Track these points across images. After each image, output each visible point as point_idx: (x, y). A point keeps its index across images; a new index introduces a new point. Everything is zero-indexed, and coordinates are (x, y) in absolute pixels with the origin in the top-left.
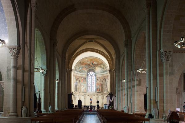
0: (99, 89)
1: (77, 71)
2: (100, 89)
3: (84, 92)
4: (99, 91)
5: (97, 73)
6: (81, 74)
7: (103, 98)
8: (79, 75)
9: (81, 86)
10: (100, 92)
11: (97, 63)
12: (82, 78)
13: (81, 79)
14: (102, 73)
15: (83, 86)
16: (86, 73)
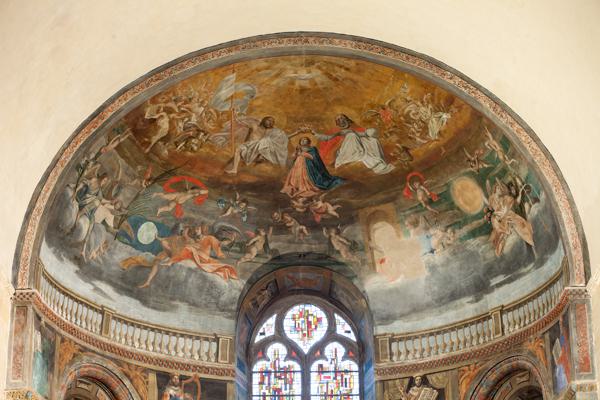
1: (89, 271)
5: (388, 319)
8: (119, 336)
11: (386, 155)
12: (164, 379)
14: (467, 308)
16: (222, 309)
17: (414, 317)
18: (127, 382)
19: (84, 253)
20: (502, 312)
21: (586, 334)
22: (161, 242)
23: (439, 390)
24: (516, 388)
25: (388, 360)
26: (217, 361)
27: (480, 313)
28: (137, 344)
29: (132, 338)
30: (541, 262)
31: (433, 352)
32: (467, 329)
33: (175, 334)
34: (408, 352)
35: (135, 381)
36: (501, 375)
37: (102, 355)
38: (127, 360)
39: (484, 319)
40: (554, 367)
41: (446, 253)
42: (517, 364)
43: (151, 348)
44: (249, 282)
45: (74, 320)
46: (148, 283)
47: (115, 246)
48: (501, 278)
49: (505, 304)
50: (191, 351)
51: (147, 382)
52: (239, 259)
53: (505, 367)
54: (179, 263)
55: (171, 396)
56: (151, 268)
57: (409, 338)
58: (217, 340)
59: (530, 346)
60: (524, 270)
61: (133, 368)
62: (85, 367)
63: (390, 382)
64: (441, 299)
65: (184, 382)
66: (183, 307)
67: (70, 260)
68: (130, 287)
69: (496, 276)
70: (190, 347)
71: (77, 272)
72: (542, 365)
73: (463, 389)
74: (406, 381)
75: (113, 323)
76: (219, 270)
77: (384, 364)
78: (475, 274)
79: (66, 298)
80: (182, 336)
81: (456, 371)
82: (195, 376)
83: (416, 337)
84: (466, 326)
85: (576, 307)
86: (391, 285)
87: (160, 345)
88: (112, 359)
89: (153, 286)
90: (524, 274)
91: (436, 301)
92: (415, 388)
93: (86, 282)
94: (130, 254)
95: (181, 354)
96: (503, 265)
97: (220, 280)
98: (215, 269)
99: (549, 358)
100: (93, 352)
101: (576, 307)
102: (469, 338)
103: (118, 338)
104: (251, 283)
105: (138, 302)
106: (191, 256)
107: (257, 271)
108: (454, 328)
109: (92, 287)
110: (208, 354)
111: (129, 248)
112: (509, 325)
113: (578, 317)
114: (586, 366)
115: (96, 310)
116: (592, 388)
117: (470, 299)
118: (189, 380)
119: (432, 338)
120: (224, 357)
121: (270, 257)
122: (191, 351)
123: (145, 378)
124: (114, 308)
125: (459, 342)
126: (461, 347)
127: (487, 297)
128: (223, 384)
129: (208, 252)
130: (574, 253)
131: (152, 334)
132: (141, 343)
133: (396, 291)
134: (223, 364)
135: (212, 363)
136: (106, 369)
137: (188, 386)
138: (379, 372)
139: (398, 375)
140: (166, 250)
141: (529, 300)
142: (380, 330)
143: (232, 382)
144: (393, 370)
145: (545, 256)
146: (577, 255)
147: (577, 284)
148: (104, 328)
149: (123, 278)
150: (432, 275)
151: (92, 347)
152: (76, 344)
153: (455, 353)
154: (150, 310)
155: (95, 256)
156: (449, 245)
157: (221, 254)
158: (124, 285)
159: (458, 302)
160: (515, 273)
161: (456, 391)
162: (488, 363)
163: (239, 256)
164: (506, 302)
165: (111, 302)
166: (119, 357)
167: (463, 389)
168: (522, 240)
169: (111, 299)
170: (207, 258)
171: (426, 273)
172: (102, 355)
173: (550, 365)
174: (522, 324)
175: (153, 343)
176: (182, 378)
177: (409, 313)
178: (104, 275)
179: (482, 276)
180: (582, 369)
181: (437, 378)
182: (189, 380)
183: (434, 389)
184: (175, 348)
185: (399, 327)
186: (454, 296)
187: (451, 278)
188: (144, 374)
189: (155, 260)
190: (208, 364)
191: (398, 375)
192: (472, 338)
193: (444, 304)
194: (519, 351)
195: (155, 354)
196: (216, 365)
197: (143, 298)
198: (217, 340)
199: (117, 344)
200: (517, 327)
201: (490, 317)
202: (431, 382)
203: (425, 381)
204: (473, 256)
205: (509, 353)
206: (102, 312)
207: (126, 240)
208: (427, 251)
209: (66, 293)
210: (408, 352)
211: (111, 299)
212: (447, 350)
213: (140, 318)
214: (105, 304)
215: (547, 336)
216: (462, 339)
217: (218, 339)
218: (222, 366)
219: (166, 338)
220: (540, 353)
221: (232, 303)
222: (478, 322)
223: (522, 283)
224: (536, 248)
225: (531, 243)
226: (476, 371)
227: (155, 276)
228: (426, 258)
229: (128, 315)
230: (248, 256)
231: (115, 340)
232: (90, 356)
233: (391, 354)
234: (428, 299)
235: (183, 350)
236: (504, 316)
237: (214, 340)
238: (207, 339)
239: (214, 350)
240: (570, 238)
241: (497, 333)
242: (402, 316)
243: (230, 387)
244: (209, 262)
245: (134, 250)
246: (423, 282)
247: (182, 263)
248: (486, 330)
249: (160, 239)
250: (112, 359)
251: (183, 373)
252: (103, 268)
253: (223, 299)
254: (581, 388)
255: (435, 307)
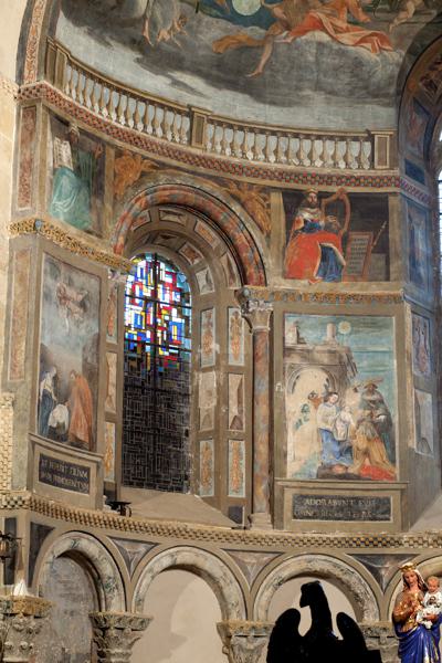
1: (157, 58)
3: (349, 509)
6: (274, 115)
8: (219, 145)
9: (269, 359)
12: (294, 200)
13: (261, 231)
15: (313, 380)
16: (374, 94)
18: (236, 208)
19: (146, 34)
22: (270, 11)
26: (372, 167)
28: (250, 155)
29: (242, 146)
33: (308, 137)
35: (249, 205)
37: (193, 173)
38: (235, 177)
43: (272, 158)
44: (410, 52)
45: (131, 123)
46: (260, 69)
47: (200, 21)
50: (333, 157)
51: (269, 206)
52: (391, 22)
54: (304, 38)
55: (306, 221)
56: (261, 47)
58: (370, 138)
61: (245, 187)
62: (164, 189)
65: (324, 201)
66: (319, 98)
67: (124, 44)
68: (231, 77)
70: (331, 153)
71: (138, 61)
75: (210, 129)
76: (363, 40)
79: (124, 97)
80: (319, 137)
82: (342, 191)
87: (286, 154)
88: (210, 177)
89: (268, 73)
93: (157, 74)
94: (226, 30)
95: (319, 163)
97: (366, 53)
98: (358, 39)
100: (177, 168)
103: (219, 148)
104: (415, 53)
105: (247, 96)
106: (320, 26)
107: (420, 37)
109: (169, 81)
110: (358, 159)
111: (223, 23)
115: (179, 112)
118: (333, 198)
120: (383, 162)
121: (435, 12)
122: (333, 157)
123: (265, 199)
124: (209, 108)
128: (384, 198)
129: (345, 16)
131: (273, 140)
132: (258, 154)
134: (381, 170)
135: (366, 171)
136: (199, 191)
137: (331, 205)
140: (281, 20)
143: (395, 194)
148: (195, 135)
149: (220, 64)
151: (175, 163)
152: (145, 158)
154: (267, 106)
155: (167, 37)
157: (362, 17)
158: (222, 75)
163: (391, 16)
165: (203, 100)
166: (221, 174)
169: (200, 94)
170: (345, 25)
172: (193, 173)
175: (276, 152)
176: (321, 195)
178: (187, 64)
182: (333, 198)
184: (310, 156)
188: (262, 194)
189: (268, 36)
190: (358, 173)
195: (279, 166)
196: (372, 173)
197: (254, 90)
198: (370, 138)
199: (218, 156)
206: (190, 114)
207: (214, 12)
209: (121, 89)
211: (200, 94)
213: (253, 118)
214: (195, 104)
217: (373, 136)
218: (379, 173)
219: (294, 144)
221: (390, 84)
227: (268, 61)
229: (232, 115)
230: (402, 15)
231: (215, 151)
232: (173, 175)
235: (321, 157)
237: (366, 140)
238: (356, 139)
239: (367, 153)
243: (393, 201)
244: (348, 30)
245: (230, 25)
247: (308, 36)
249: (269, 6)
250: (210, 177)
251: (324, 188)
252: (183, 53)
253: (374, 80)
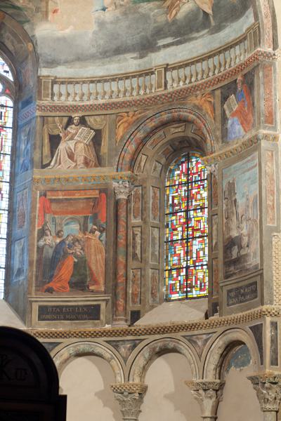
0: (81, 266)
2: (97, 263)
4: (79, 299)
5: (52, 63)
7: (143, 390)
10: (92, 313)
14: (131, 63)
17: (78, 64)
20: (166, 69)
21: (271, 92)
23: (95, 130)
24: (169, 137)
25: (49, 99)
27: (143, 68)
30: (218, 28)
31: (92, 97)
32: (128, 82)
34: (68, 94)
36: (160, 124)
39: (147, 74)
40: (224, 119)
41: (118, 12)
42: (179, 115)
48: (169, 40)
49: (170, 63)
53: (165, 117)
57: (71, 83)
59: (195, 100)
60: (196, 35)
63: (50, 119)
64: (106, 52)
69: (163, 38)
72: (209, 118)
73: (120, 131)
74: (65, 120)
77: (46, 102)
78: (143, 33)
81: (114, 116)
83: (77, 83)
84: (127, 78)
85: (265, 67)
86: (60, 34)
90: (196, 38)
91: (101, 54)
92: (73, 126)
96: (173, 28)
99: (218, 112)
101: (265, 67)
102: (129, 89)
108: (115, 78)
112: (173, 80)
113: (266, 76)
114: (270, 119)
116: (275, 138)
117: (135, 55)
119: (92, 85)
125: (119, 91)
126: (121, 95)
127: (153, 55)
130: (265, 21)
133: (63, 40)
138: (41, 108)
139: (58, 113)
141: (198, 61)
142: (44, 72)
144: (55, 108)
145: (224, 24)
146: (267, 23)
147: (266, 48)
150: (100, 30)
153: (114, 100)
156: (121, 5)
159: (122, 56)
160: (186, 37)
161: (113, 132)
162: (148, 112)
164: (171, 61)
167: (120, 131)
168: (199, 8)
171: (95, 27)
173: (219, 118)
174: (187, 81)
177: (73, 61)
179: (149, 38)
180: (266, 122)
181: (95, 120)
183: (92, 129)
185: (62, 72)
186: (119, 51)
187: (118, 35)
191: (58, 113)
192: (132, 89)
193: (107, 57)
194: (183, 104)
200: (181, 83)
201: (152, 73)
202: (89, 123)
203: (83, 121)
204: (145, 17)
205: (171, 105)
208: (100, 8)
210: (68, 94)
212: (107, 97)
215: (218, 93)
216: (122, 90)
220: (207, 107)
222: (140, 76)
223: (192, 46)
224: (214, 17)
225: (209, 11)
226: (134, 118)
228: (97, 14)
233: (53, 95)
234: (93, 50)
236: (168, 74)
240: (262, 7)
241: (159, 87)
242: (66, 62)
246: (90, 35)
248: (148, 84)
254: (266, 137)
255: (100, 58)
